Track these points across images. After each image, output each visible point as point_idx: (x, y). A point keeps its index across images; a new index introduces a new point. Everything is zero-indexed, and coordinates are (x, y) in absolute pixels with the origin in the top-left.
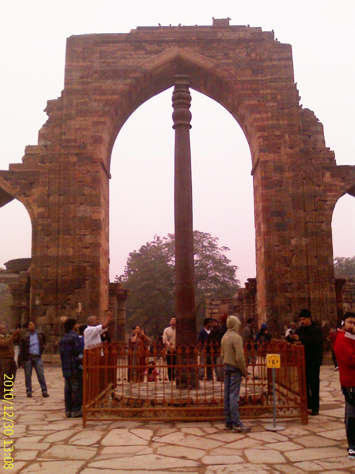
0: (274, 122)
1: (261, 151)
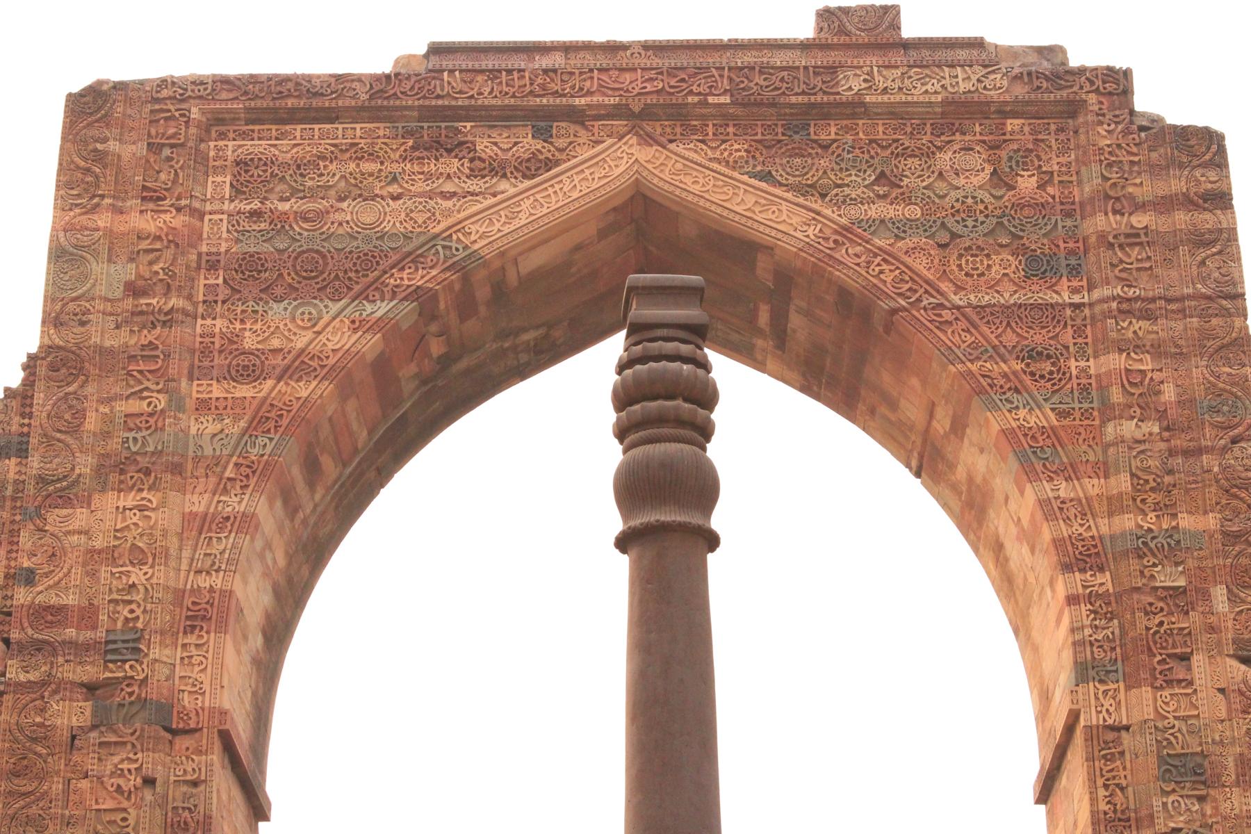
1: (1085, 671)
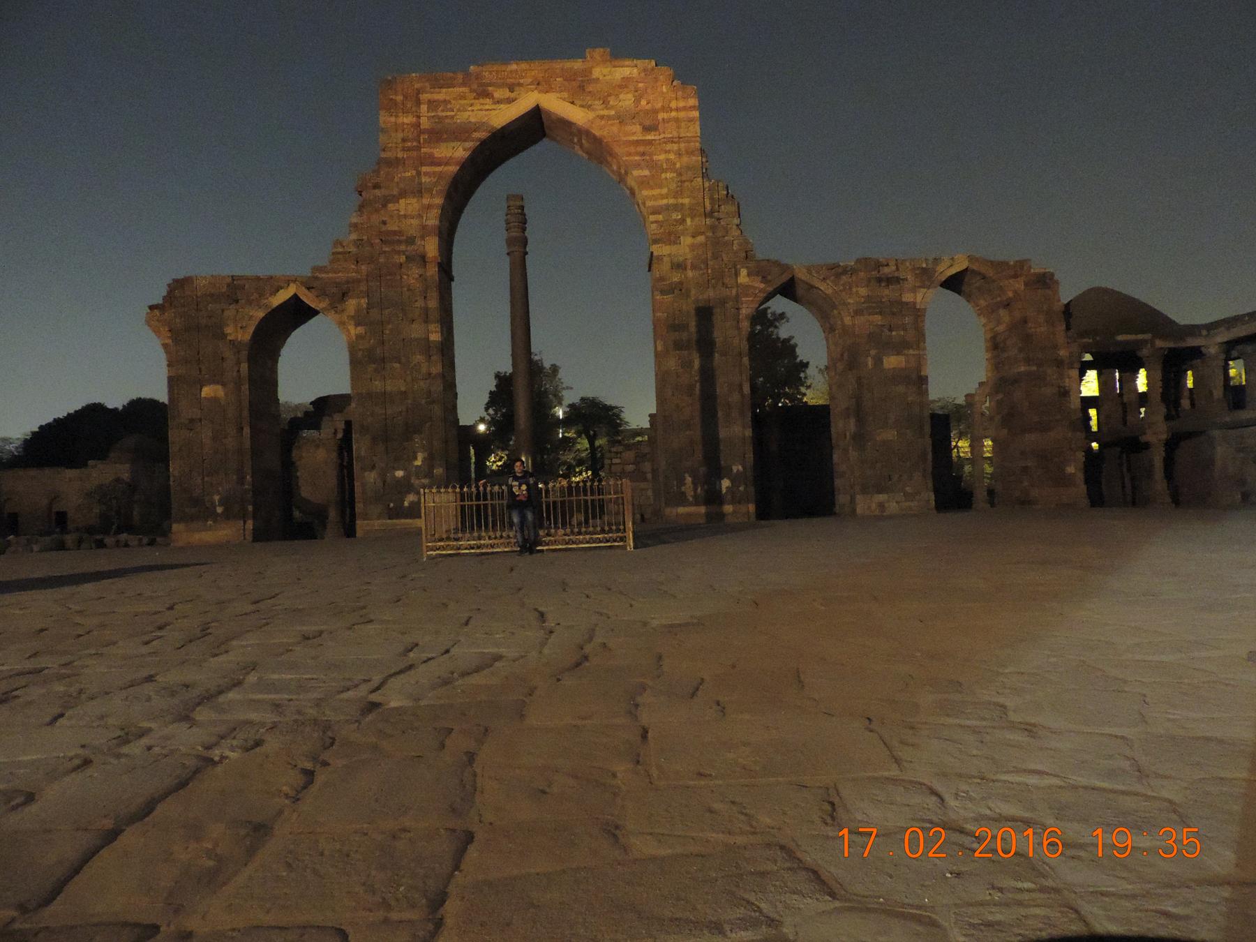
0: (672, 201)
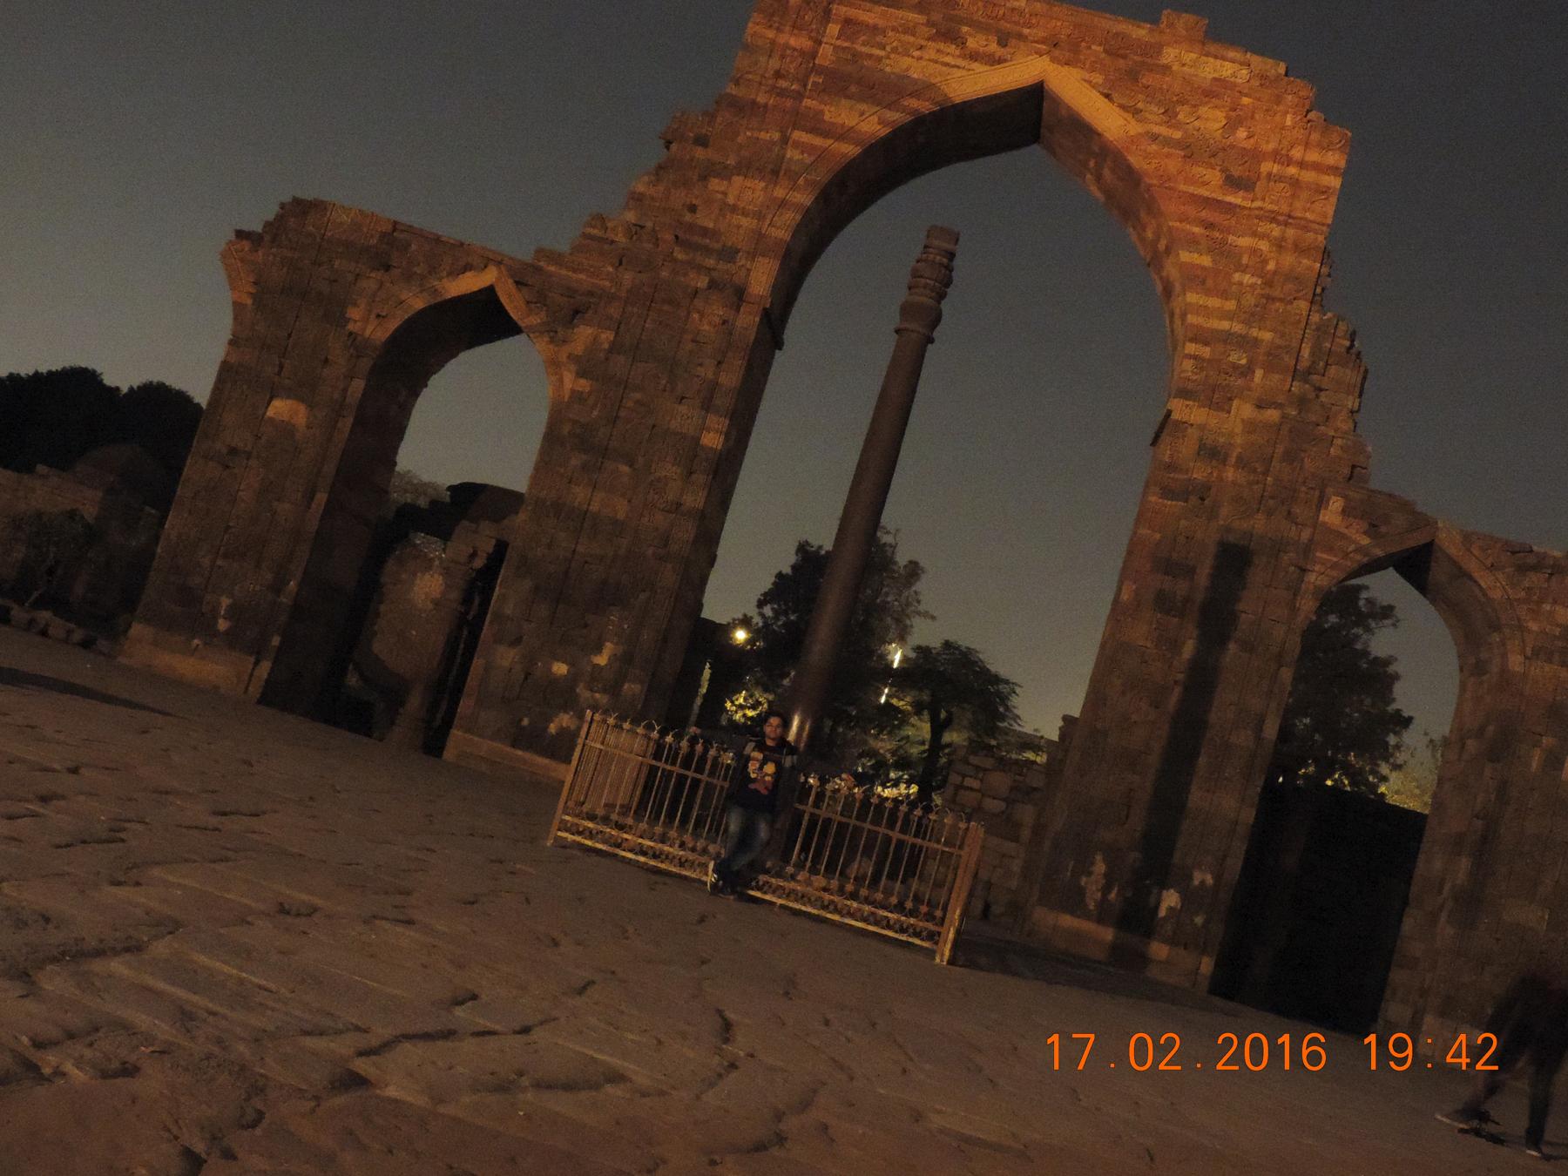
0: (1237, 328)
